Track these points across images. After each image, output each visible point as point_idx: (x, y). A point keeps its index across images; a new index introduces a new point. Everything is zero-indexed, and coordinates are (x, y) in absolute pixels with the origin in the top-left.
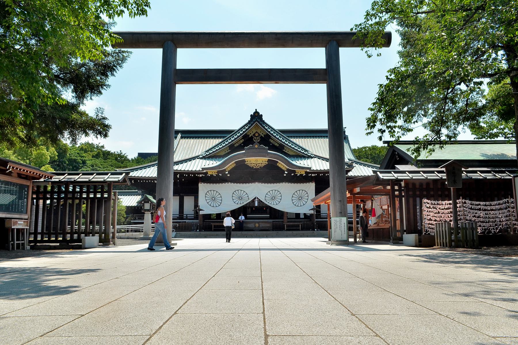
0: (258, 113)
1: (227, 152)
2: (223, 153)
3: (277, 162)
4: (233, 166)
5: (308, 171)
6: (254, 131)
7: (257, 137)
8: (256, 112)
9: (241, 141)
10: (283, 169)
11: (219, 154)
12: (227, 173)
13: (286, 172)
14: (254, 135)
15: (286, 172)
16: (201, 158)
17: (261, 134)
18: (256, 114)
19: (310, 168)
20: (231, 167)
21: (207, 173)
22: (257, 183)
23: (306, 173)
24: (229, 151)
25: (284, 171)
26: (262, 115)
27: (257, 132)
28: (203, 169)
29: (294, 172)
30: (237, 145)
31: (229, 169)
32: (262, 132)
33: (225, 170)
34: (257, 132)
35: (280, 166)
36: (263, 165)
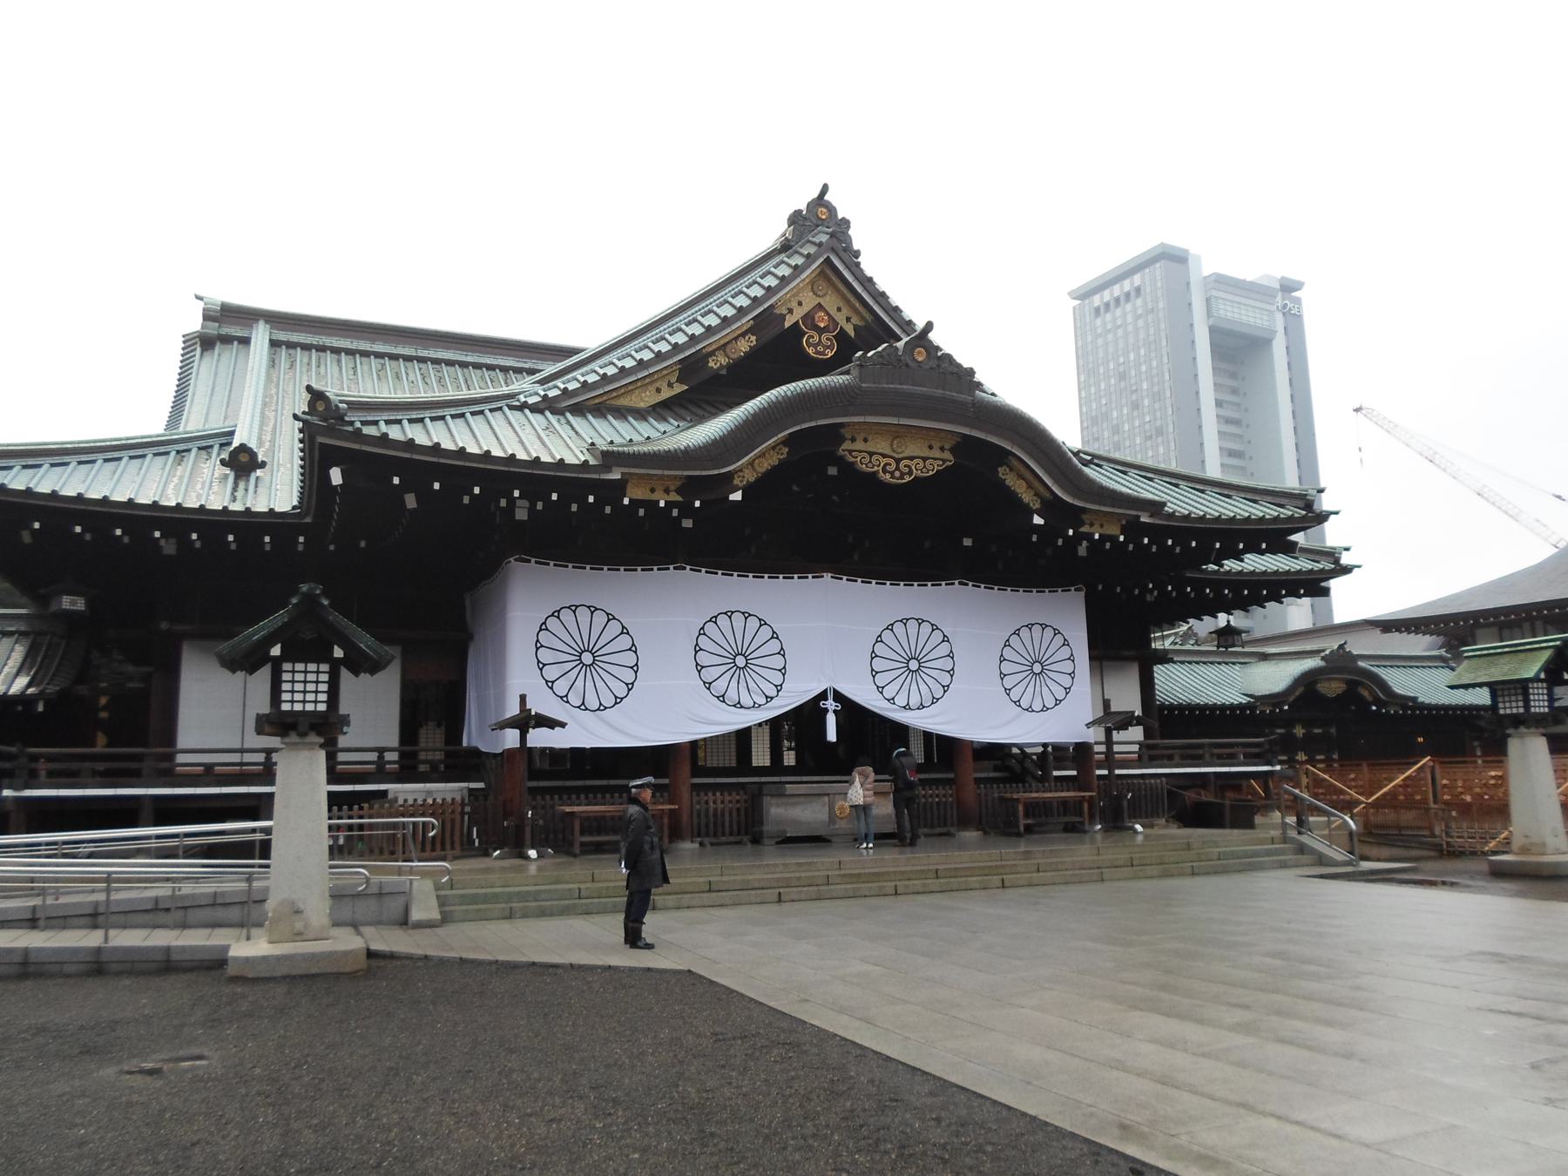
0: (831, 210)
1: (666, 394)
2: (648, 399)
3: (1002, 456)
4: (774, 460)
5: (1145, 519)
6: (809, 302)
7: (820, 331)
8: (820, 200)
9: (744, 346)
10: (1027, 497)
11: (624, 402)
12: (737, 496)
13: (1037, 520)
14: (809, 318)
15: (1037, 520)
16: (535, 409)
17: (840, 318)
18: (823, 213)
19: (1156, 507)
20: (764, 466)
21: (620, 487)
22: (827, 576)
23: (1133, 528)
24: (679, 388)
25: (1030, 513)
26: (846, 223)
27: (820, 307)
28: (610, 458)
29: (1074, 515)
30: (723, 361)
31: (750, 477)
32: (846, 311)
33: (726, 481)
34: (820, 307)
35: (1011, 481)
36: (933, 468)
